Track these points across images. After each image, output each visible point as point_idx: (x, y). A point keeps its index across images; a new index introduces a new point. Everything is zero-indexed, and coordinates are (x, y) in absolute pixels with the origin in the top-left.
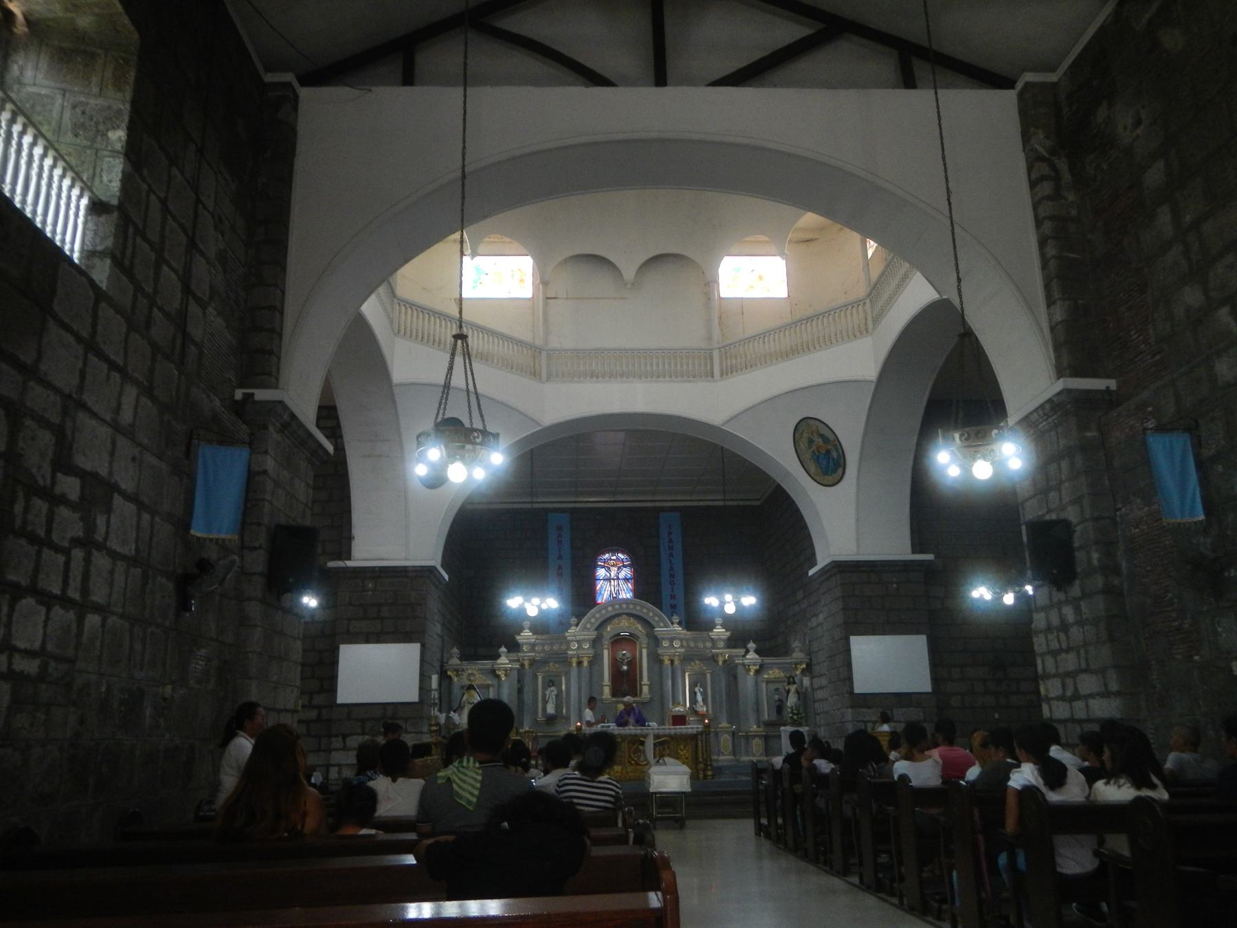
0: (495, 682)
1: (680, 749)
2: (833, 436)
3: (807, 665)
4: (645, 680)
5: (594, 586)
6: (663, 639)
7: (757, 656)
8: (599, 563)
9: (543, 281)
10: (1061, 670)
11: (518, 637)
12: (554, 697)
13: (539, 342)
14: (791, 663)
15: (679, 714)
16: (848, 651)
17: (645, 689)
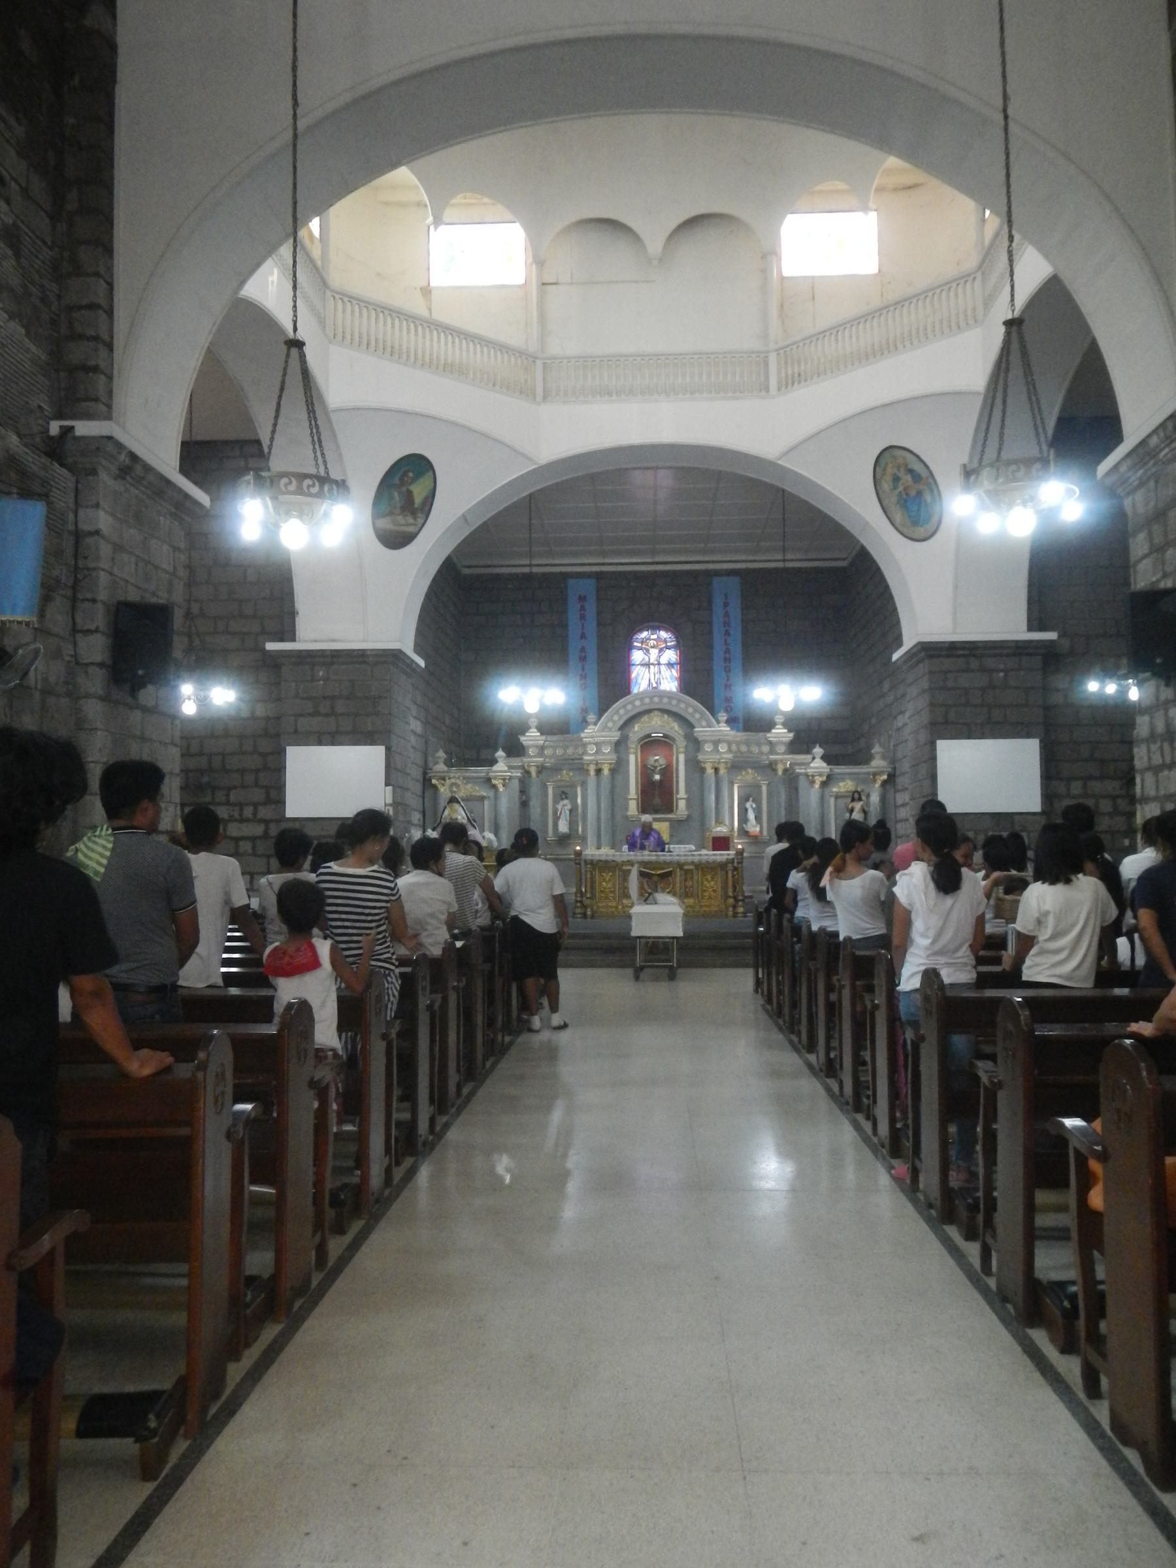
0: (491, 794)
1: (707, 880)
3: (889, 776)
4: (682, 793)
5: (629, 673)
6: (706, 742)
7: (825, 765)
8: (635, 644)
9: (538, 261)
10: (1162, 792)
11: (522, 739)
12: (568, 812)
13: (533, 348)
14: (868, 773)
15: (722, 835)
16: (933, 758)
17: (682, 804)
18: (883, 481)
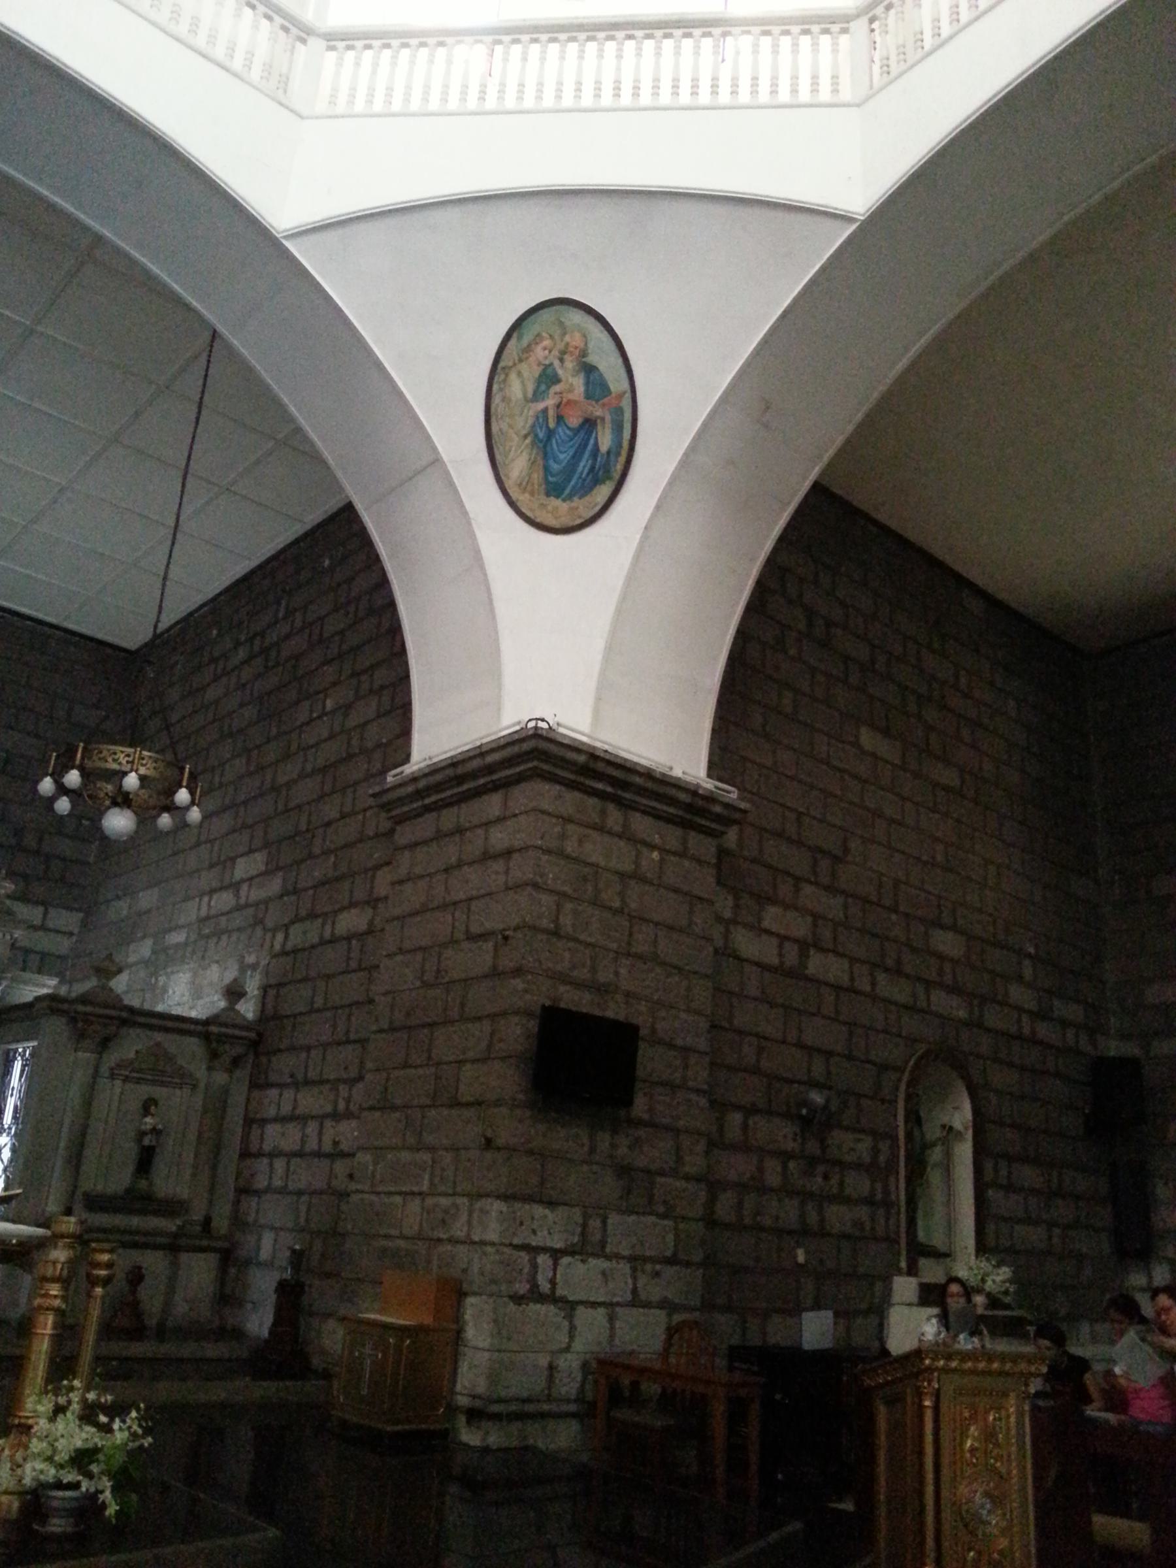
2: (624, 374)
18: (513, 376)
